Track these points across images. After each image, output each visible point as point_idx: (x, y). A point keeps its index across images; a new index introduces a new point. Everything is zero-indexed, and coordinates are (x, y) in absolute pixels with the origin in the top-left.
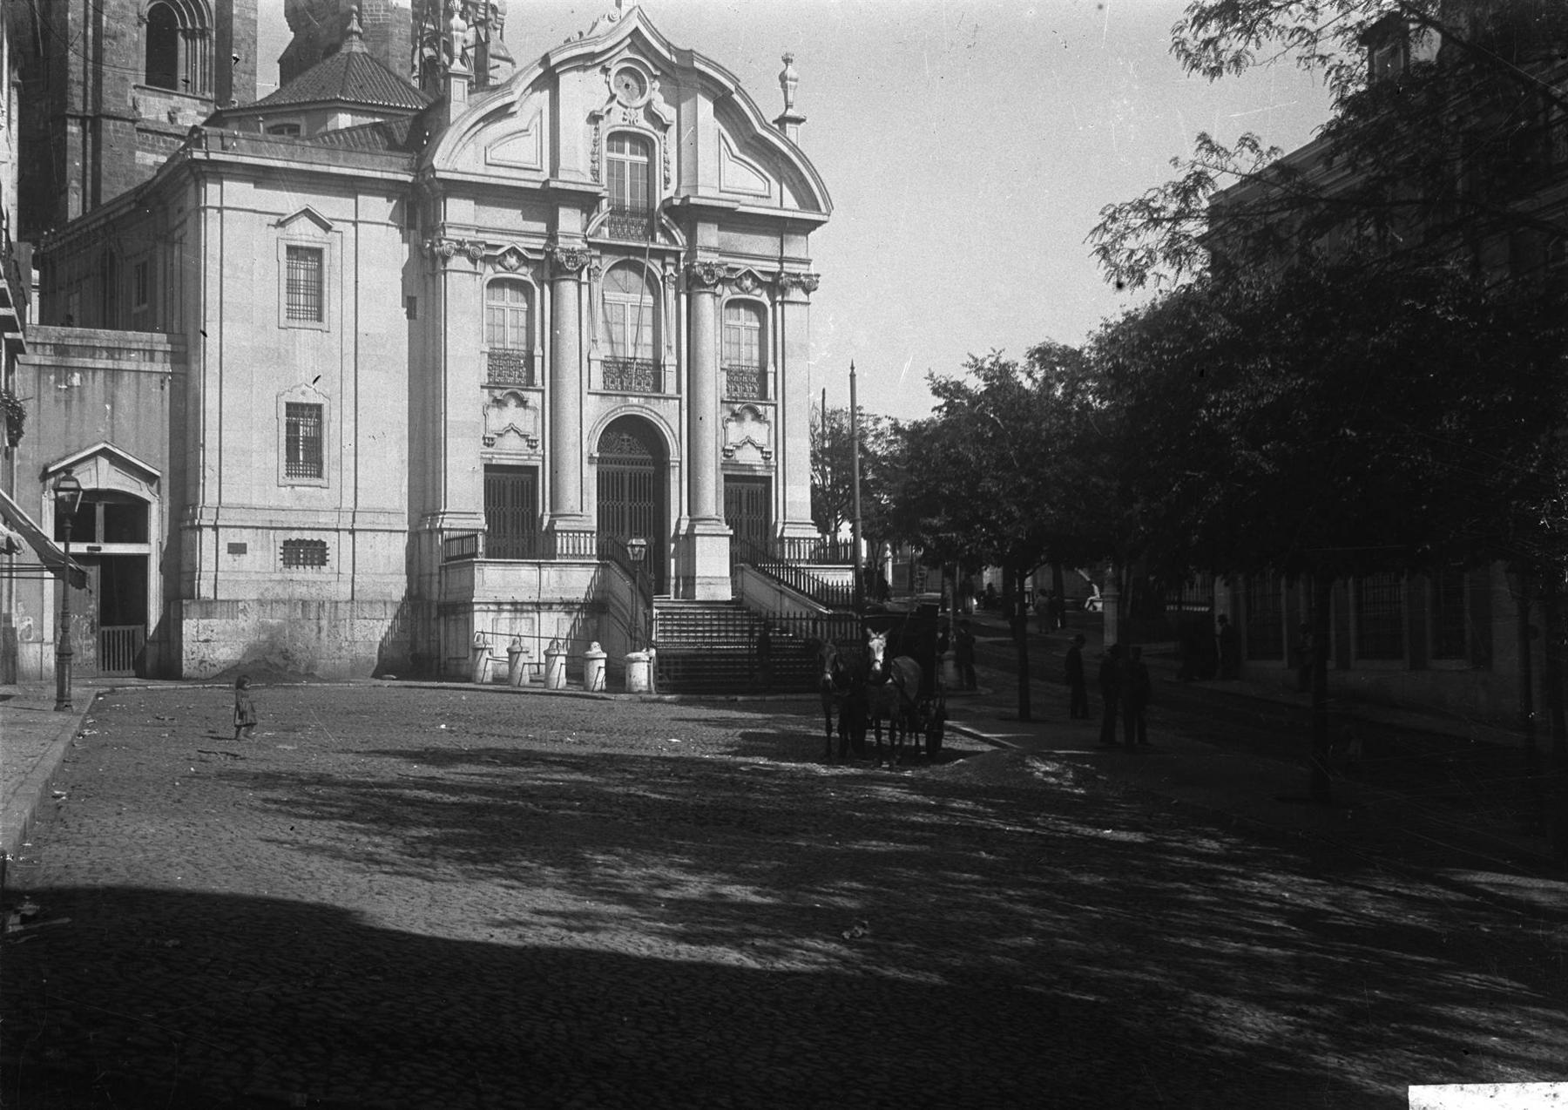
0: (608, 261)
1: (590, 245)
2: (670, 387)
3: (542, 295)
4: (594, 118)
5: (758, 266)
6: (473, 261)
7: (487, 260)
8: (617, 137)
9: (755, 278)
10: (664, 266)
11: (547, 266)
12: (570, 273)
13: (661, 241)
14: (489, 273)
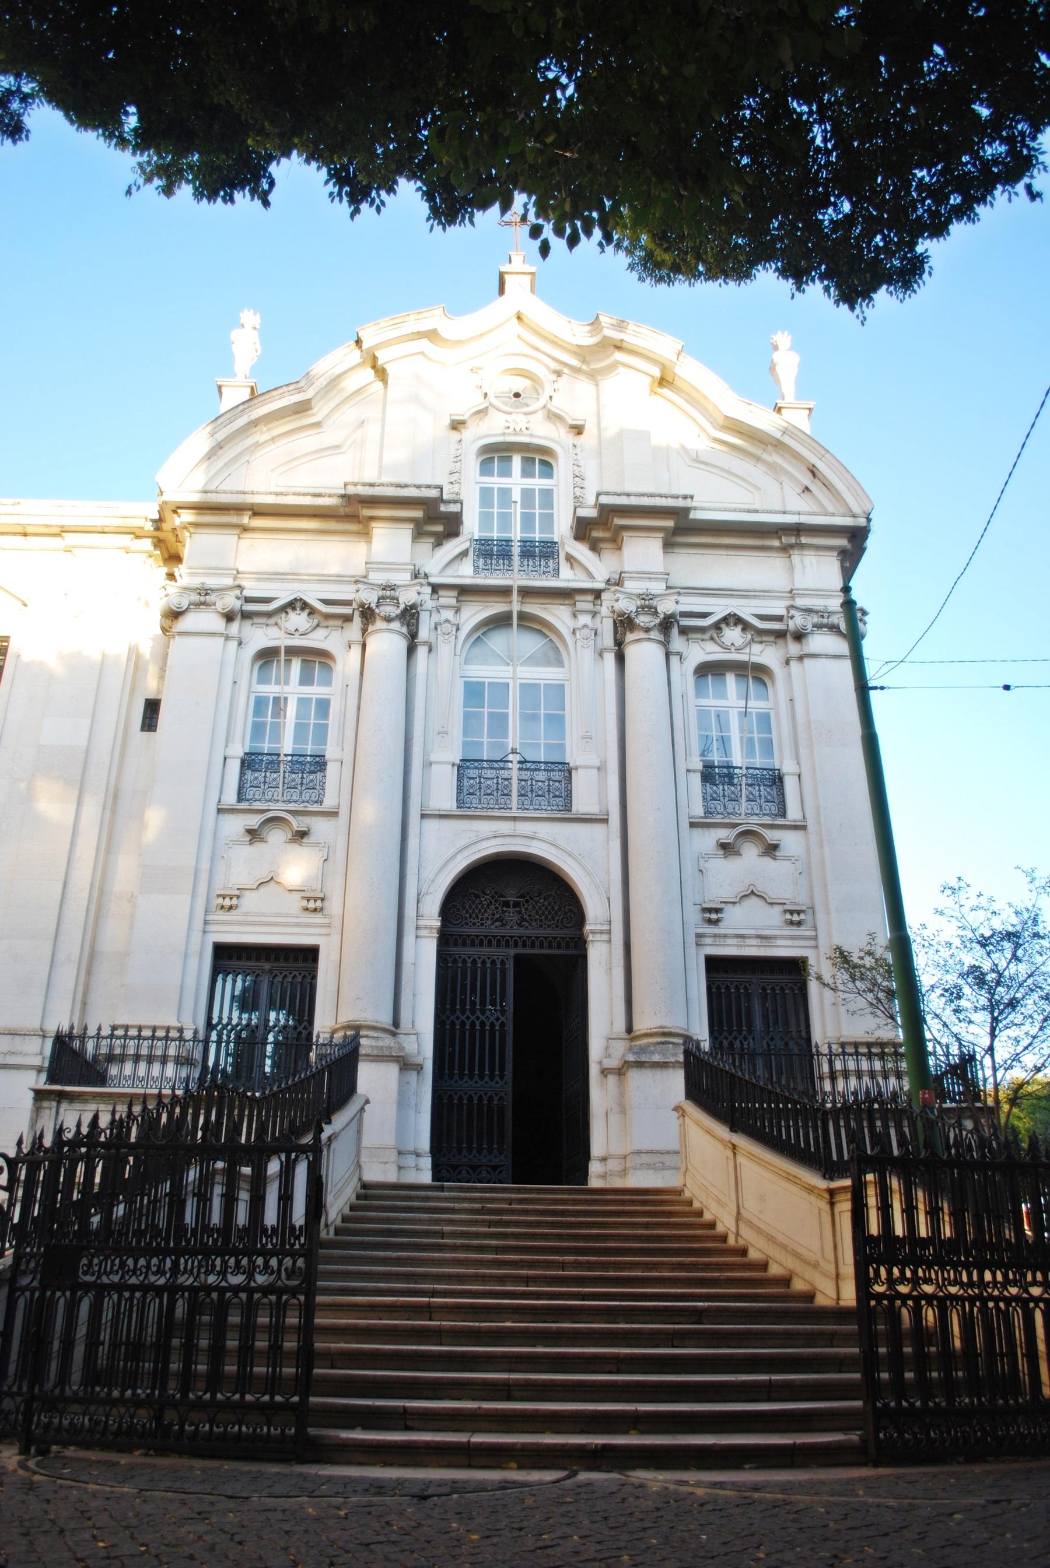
0: (475, 613)
1: (436, 588)
2: (583, 802)
3: (347, 663)
4: (456, 425)
5: (747, 610)
6: (229, 617)
7: (246, 616)
8: (496, 454)
9: (746, 626)
10: (575, 616)
11: (357, 620)
12: (388, 619)
13: (567, 577)
14: (261, 636)
